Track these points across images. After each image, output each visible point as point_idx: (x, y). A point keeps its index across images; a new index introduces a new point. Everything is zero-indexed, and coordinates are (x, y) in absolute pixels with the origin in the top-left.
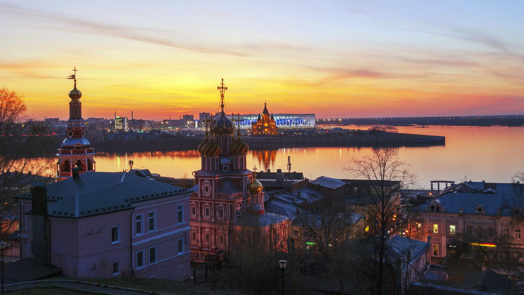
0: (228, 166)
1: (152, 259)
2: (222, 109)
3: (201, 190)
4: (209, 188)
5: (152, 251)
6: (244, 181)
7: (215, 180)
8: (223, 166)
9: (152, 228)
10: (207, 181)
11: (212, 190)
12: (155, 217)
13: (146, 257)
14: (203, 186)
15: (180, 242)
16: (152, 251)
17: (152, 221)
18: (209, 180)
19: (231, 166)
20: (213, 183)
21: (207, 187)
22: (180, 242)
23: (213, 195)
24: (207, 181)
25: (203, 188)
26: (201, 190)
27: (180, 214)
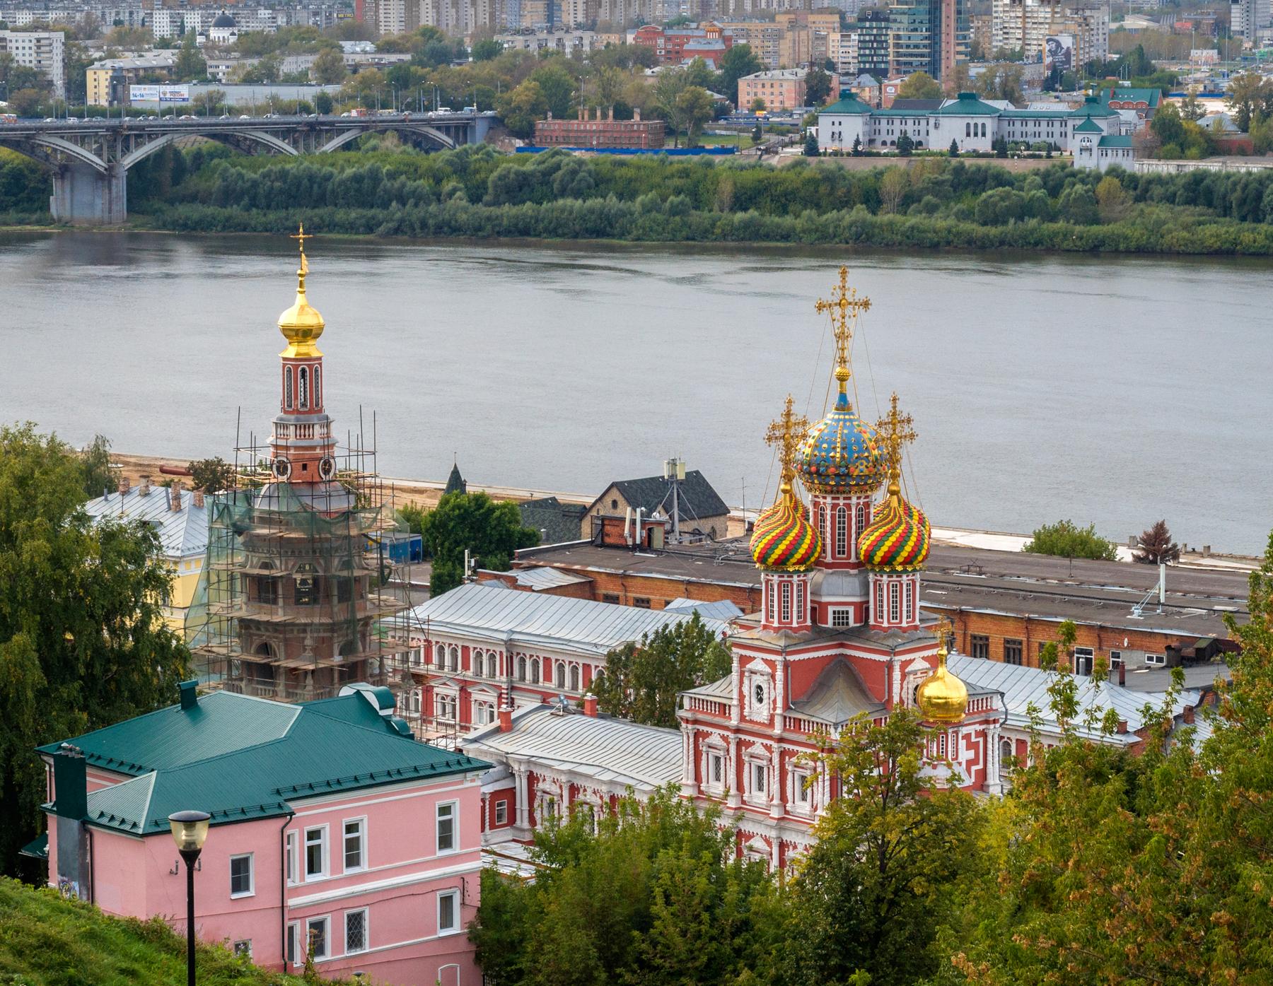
0: (851, 610)
1: (355, 939)
2: (841, 386)
3: (741, 697)
4: (765, 691)
5: (355, 922)
6: (897, 675)
7: (786, 665)
8: (831, 609)
9: (352, 861)
10: (758, 665)
11: (775, 701)
12: (363, 833)
13: (335, 932)
14: (746, 681)
15: (447, 901)
16: (355, 922)
17: (353, 845)
18: (765, 661)
19: (862, 610)
20: (779, 674)
21: (759, 687)
22: (447, 901)
23: (778, 722)
24: (758, 665)
25: (746, 692)
26: (741, 697)
27: (446, 827)
